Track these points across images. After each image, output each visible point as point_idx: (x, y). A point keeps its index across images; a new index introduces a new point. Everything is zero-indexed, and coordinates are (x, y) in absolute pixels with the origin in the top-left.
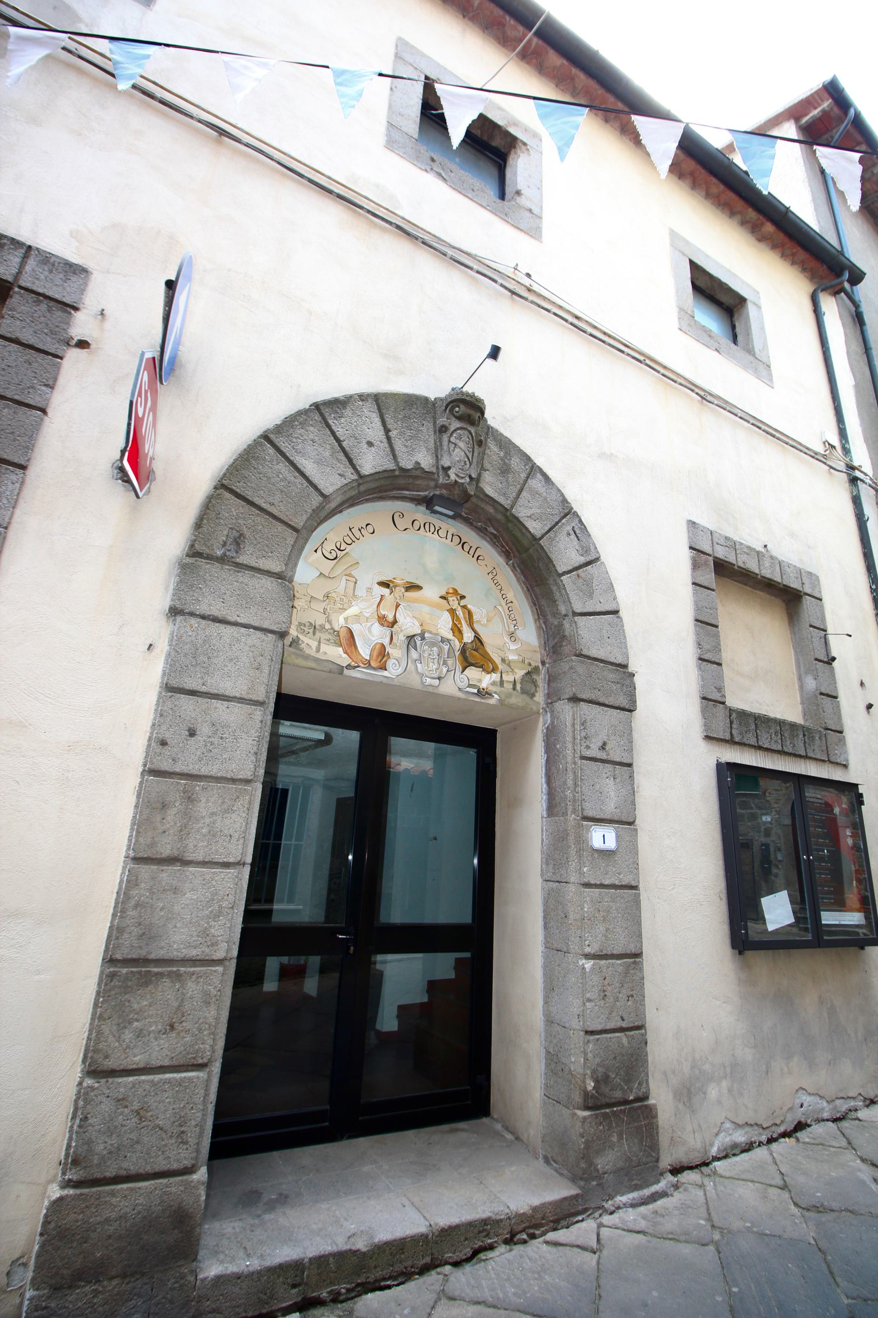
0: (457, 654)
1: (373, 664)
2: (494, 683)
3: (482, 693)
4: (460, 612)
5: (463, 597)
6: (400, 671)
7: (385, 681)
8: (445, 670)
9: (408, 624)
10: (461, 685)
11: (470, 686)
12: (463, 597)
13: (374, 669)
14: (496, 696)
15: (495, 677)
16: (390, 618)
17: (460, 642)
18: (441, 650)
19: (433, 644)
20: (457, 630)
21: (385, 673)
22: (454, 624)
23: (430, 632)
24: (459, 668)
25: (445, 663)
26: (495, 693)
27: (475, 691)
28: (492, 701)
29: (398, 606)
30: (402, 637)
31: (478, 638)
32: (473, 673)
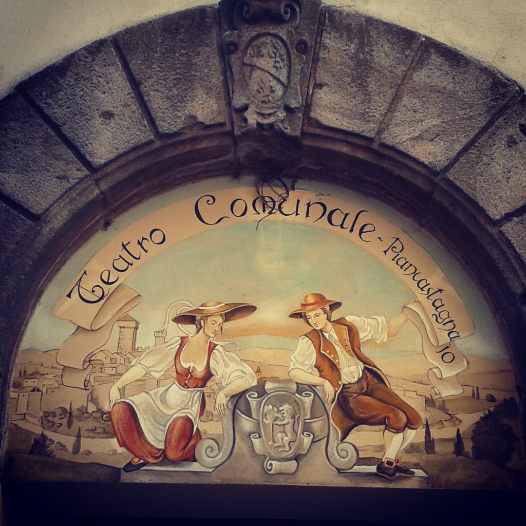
0: (330, 408)
1: (171, 455)
2: (412, 449)
3: (385, 470)
4: (331, 333)
5: (335, 306)
6: (221, 457)
7: (193, 480)
8: (307, 440)
9: (232, 374)
10: (342, 463)
11: (360, 461)
12: (335, 306)
13: (174, 463)
14: (419, 473)
15: (414, 436)
16: (200, 370)
17: (334, 384)
18: (297, 406)
19: (280, 400)
20: (328, 366)
21: (195, 467)
22: (321, 356)
23: (275, 380)
24: (336, 431)
25: (307, 428)
26: (417, 466)
27: (373, 469)
28: (410, 484)
29: (212, 348)
30: (222, 399)
31: (371, 373)
32: (365, 437)
